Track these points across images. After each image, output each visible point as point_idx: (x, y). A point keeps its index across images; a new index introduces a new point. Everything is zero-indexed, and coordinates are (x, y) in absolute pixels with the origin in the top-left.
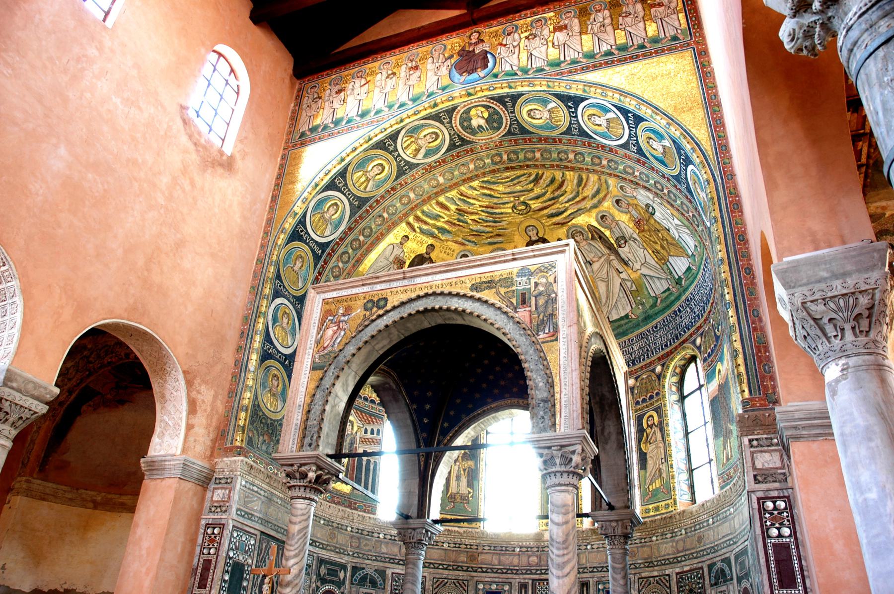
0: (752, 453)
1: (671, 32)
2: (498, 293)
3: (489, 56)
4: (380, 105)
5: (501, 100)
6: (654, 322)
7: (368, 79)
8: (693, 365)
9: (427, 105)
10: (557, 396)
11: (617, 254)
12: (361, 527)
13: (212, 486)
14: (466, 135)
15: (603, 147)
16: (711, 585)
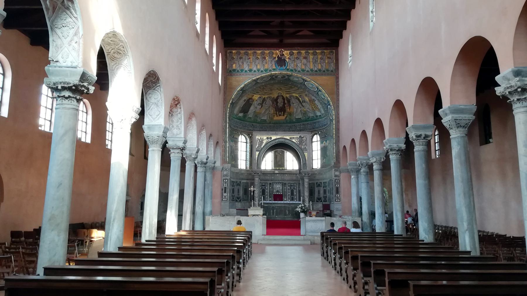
0: (335, 172)
1: (331, 69)
2: (295, 140)
3: (286, 62)
4: (255, 69)
5: (288, 76)
6: (308, 122)
7: (250, 57)
8: (316, 135)
9: (269, 73)
10: (307, 163)
11: (301, 104)
12: (237, 172)
13: (223, 171)
14: (275, 78)
15: (308, 88)
16: (316, 187)
